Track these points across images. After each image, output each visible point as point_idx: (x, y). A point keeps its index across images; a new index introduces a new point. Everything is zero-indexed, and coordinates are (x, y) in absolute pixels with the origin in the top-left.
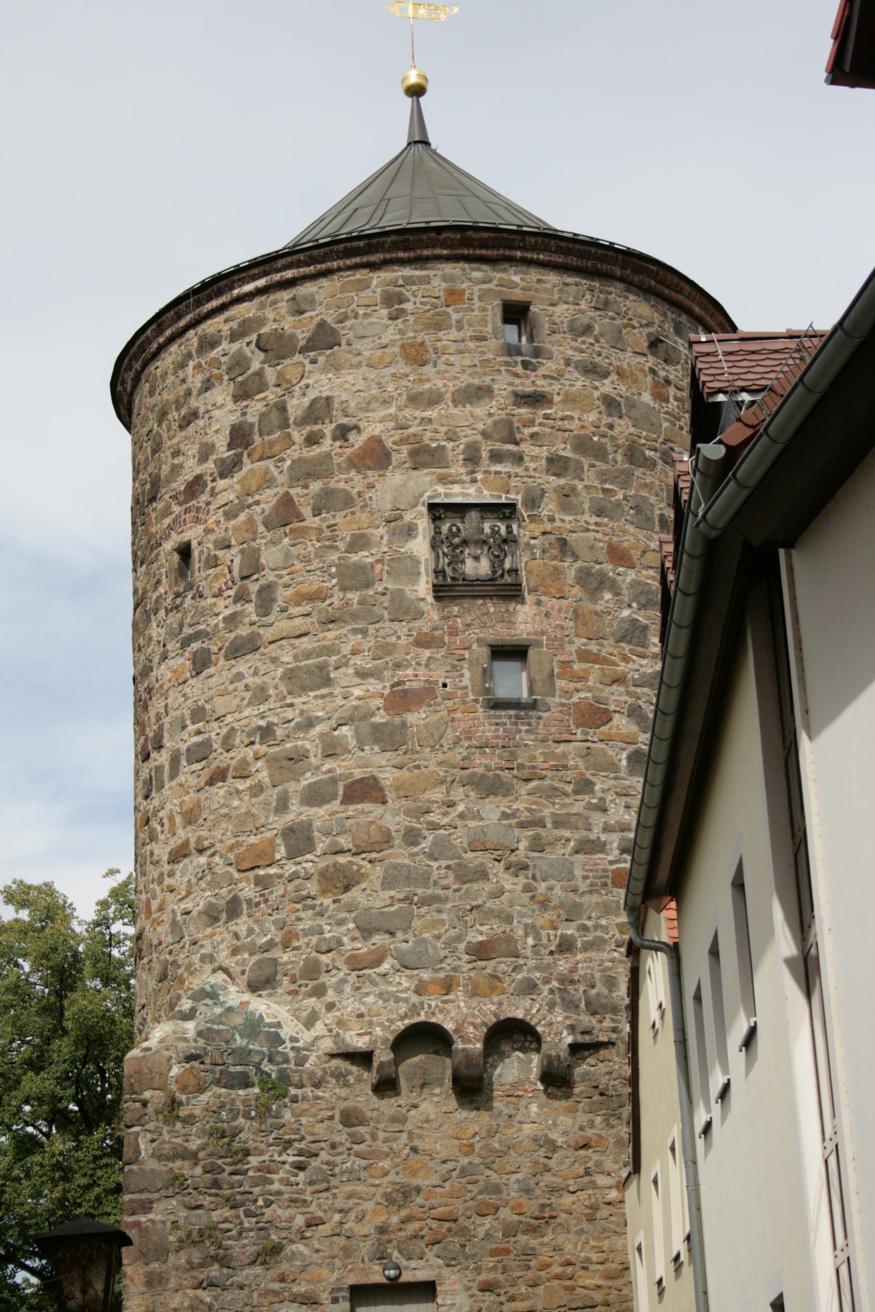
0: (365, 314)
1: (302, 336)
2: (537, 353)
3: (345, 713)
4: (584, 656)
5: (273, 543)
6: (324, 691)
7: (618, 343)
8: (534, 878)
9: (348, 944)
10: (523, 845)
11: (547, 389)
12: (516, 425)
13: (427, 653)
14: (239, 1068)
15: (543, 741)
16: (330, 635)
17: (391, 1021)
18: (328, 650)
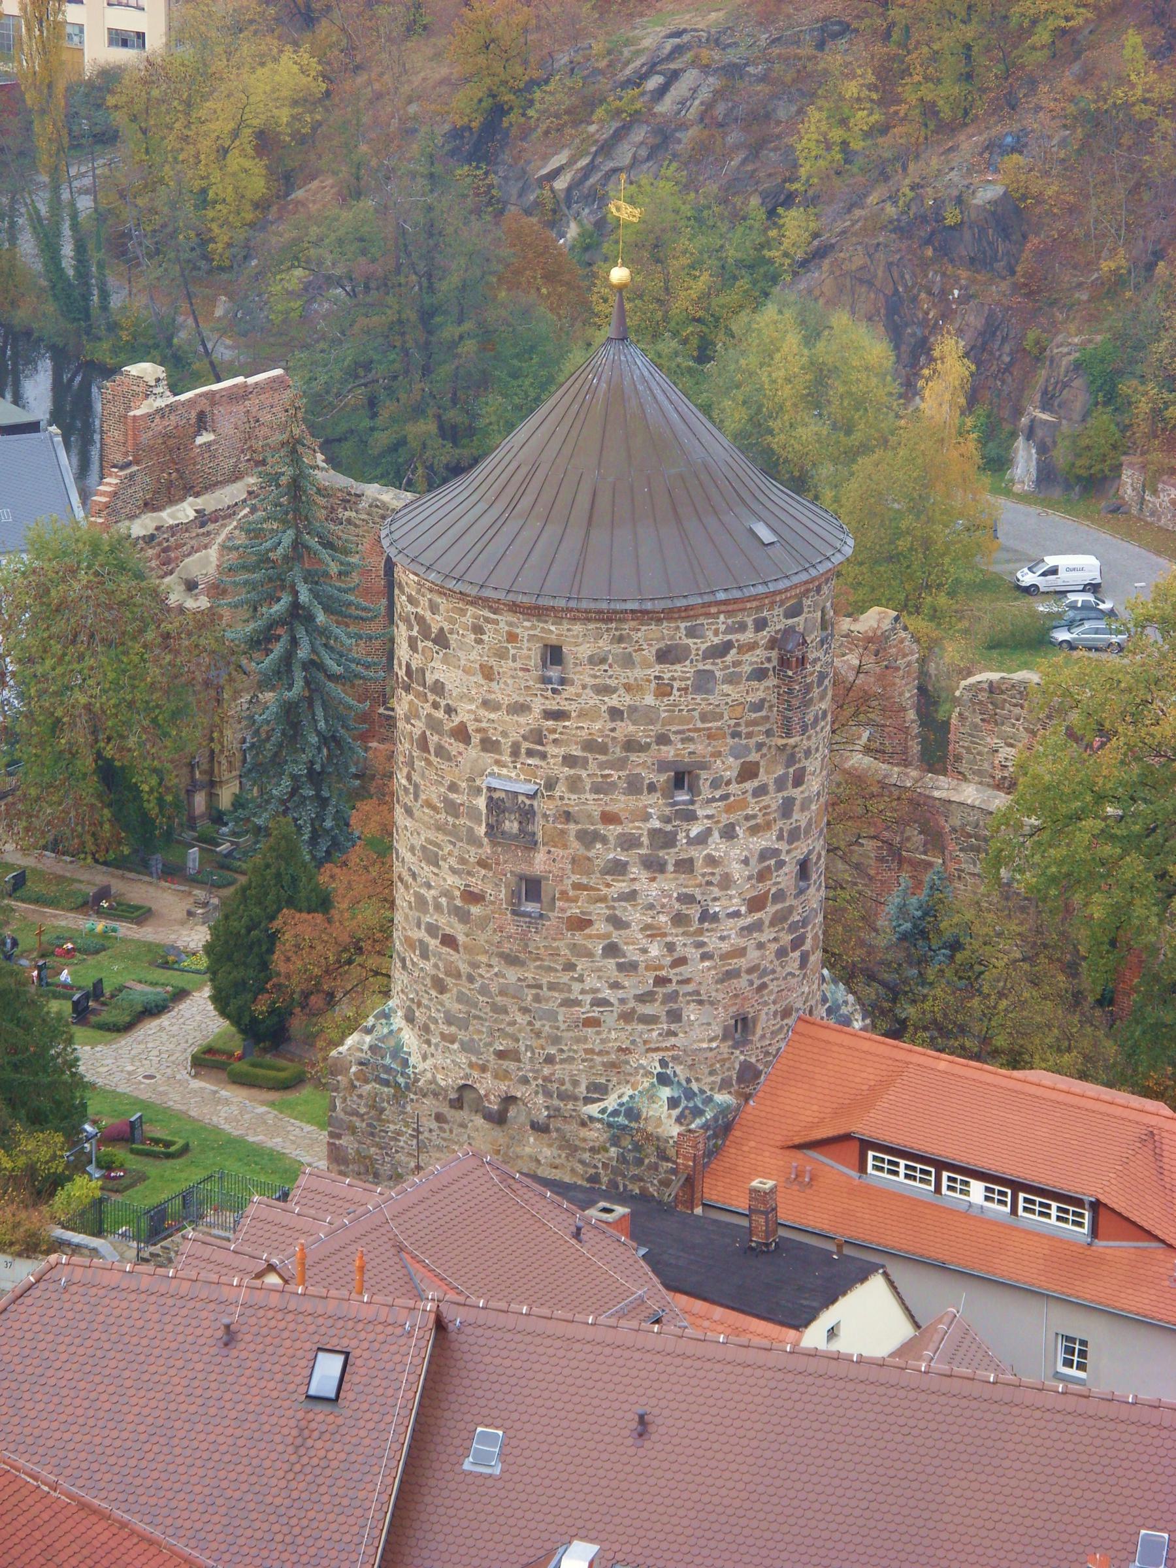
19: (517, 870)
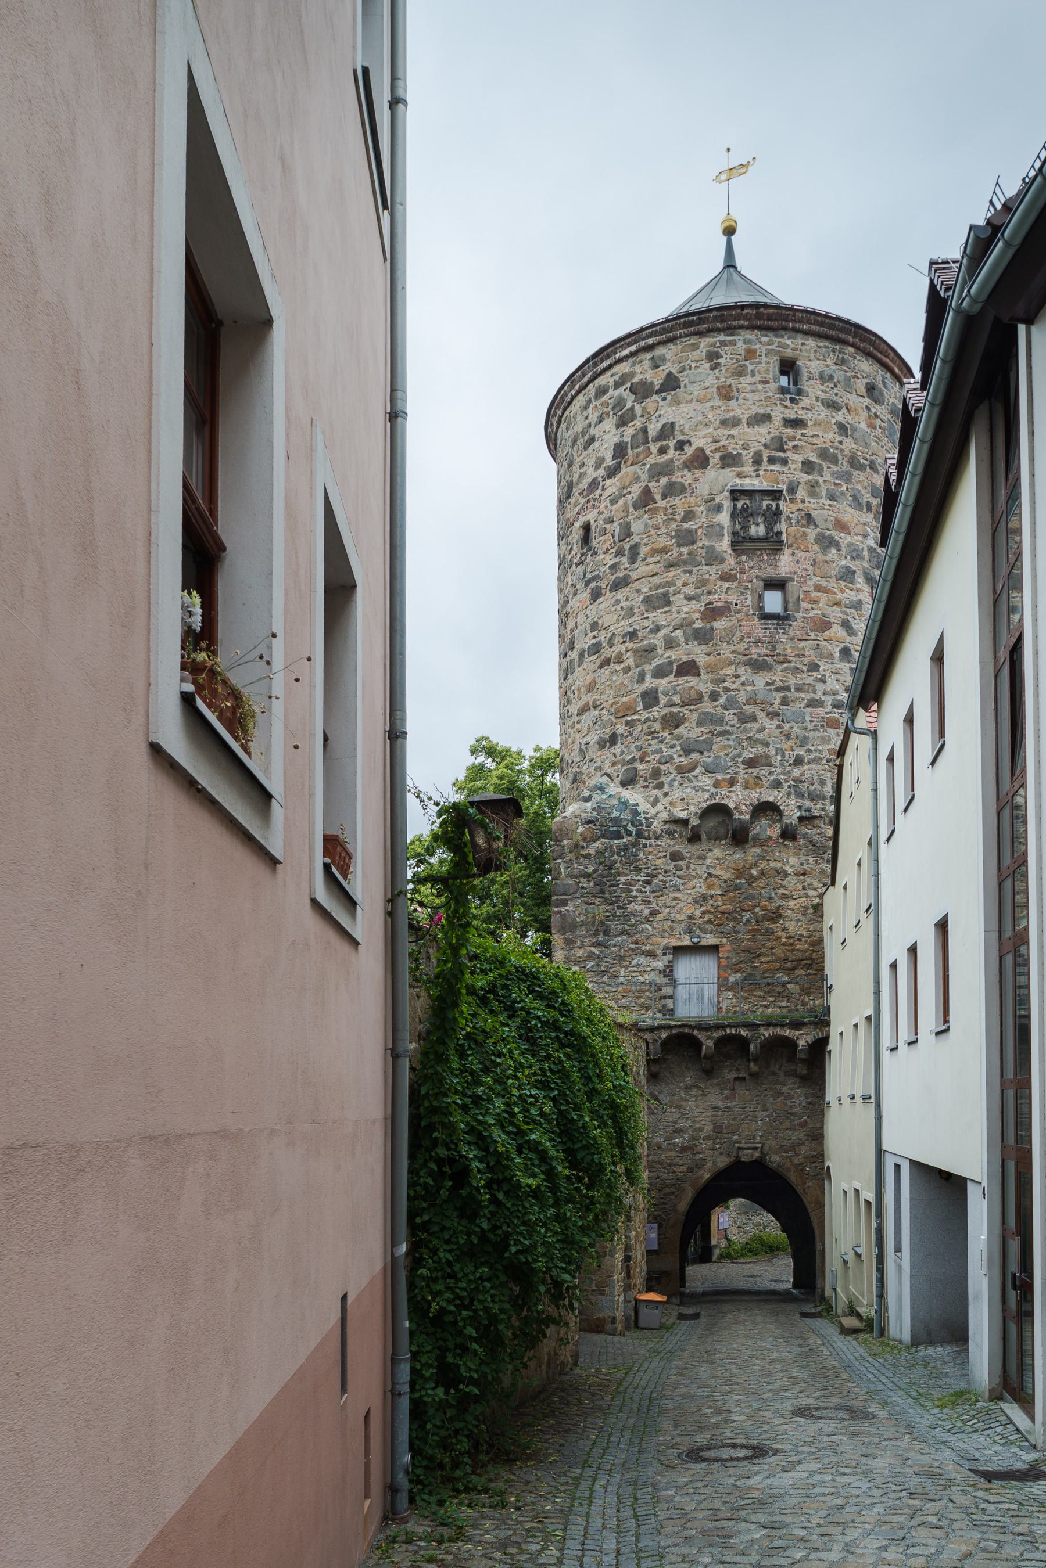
1: (657, 383)
3: (677, 622)
4: (818, 588)
5: (639, 518)
6: (666, 609)
7: (848, 386)
8: (783, 721)
9: (677, 760)
10: (777, 701)
13: (727, 585)
14: (615, 828)
15: (792, 639)
16: (671, 574)
17: (699, 802)
18: (670, 584)
19: (763, 574)
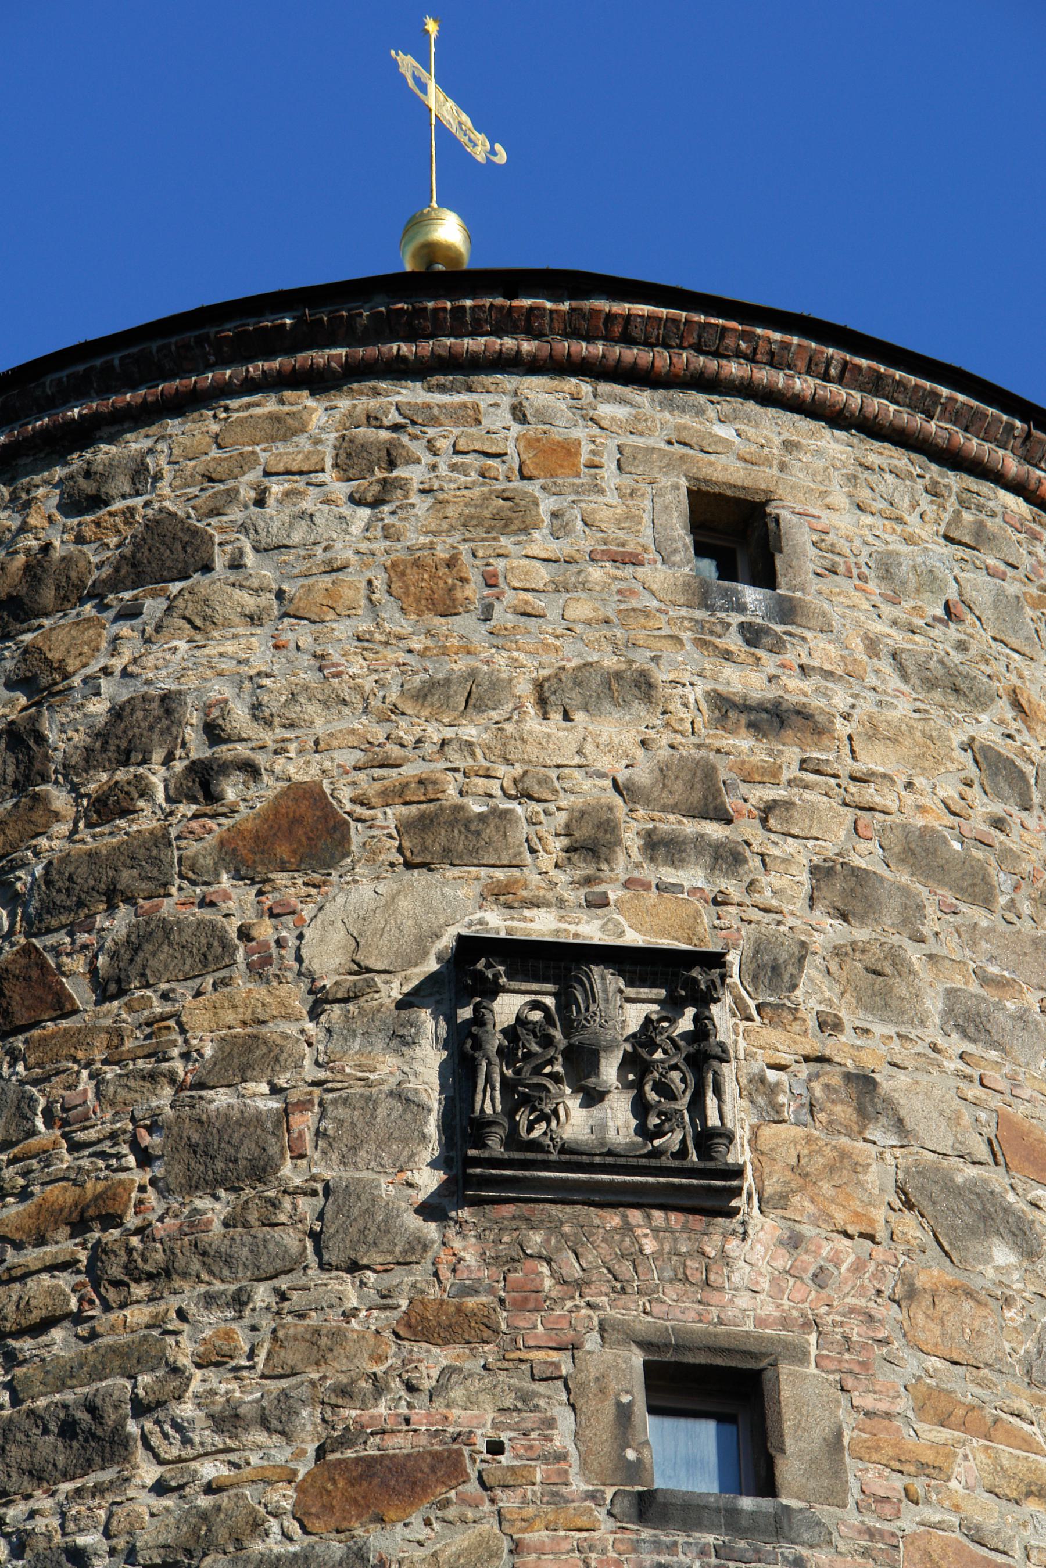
0: (287, 494)
2: (787, 611)
11: (817, 703)
12: (723, 775)
